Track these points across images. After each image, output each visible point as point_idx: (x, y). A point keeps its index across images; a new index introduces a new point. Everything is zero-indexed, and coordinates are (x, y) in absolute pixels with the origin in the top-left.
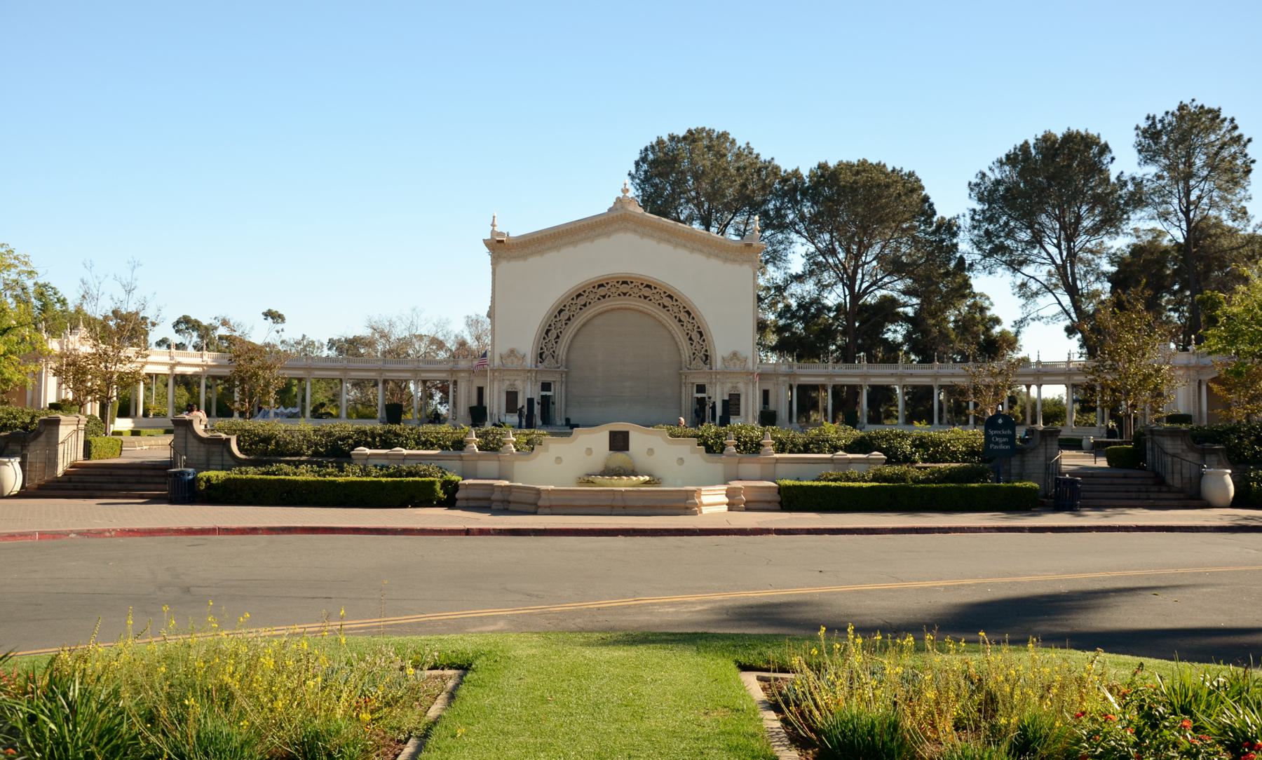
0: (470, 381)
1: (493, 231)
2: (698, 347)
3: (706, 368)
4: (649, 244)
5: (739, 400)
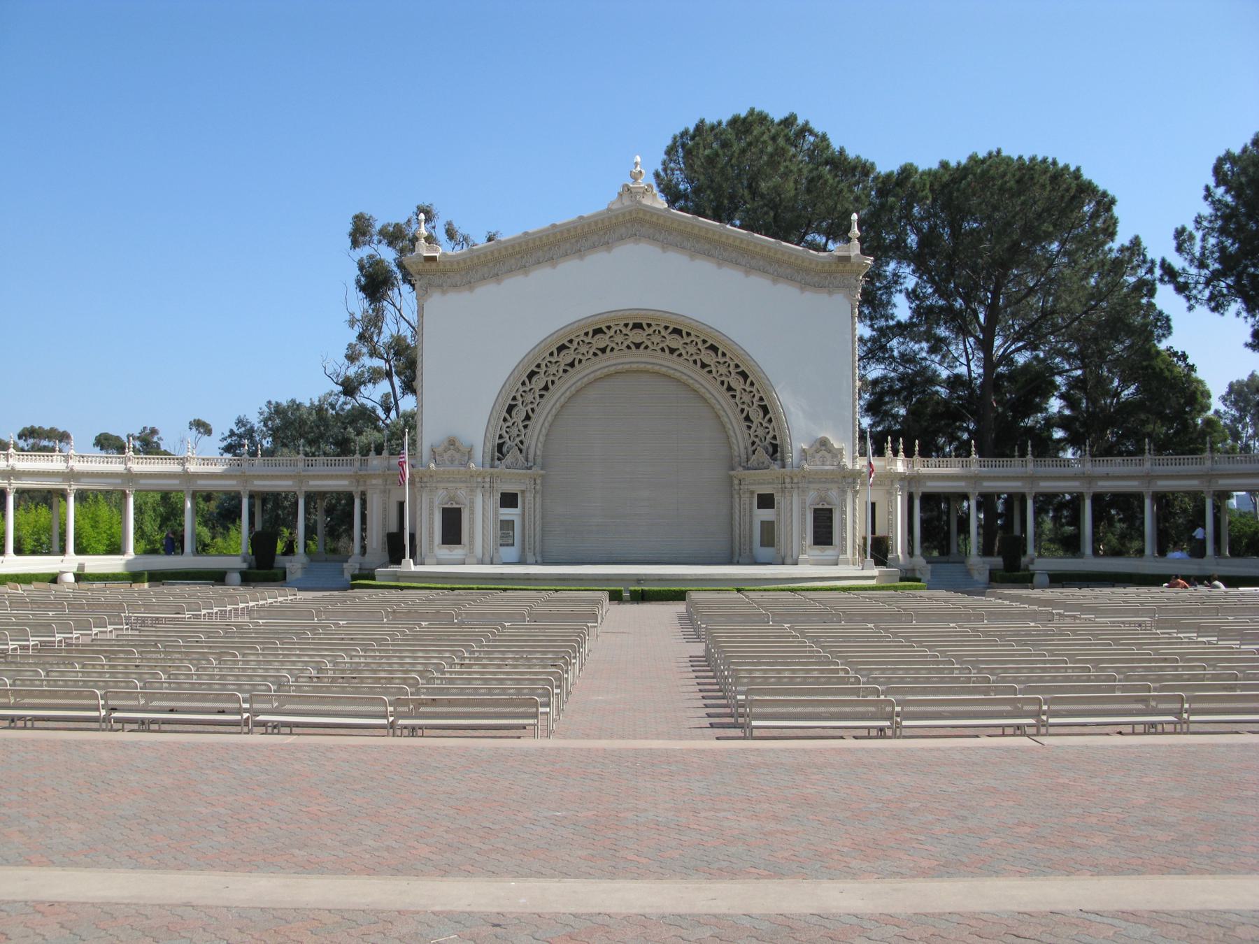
0: (385, 492)
2: (761, 432)
3: (776, 467)
4: (676, 261)
5: (830, 519)
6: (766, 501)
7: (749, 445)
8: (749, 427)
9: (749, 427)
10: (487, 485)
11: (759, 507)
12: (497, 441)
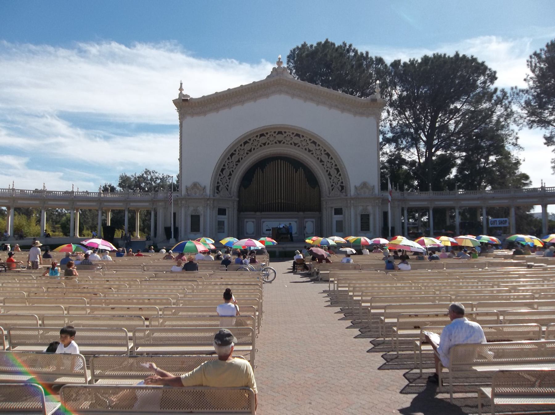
1: (181, 94)
2: (336, 180)
5: (369, 219)
6: (338, 211)
7: (330, 186)
8: (330, 178)
9: (330, 178)
10: (211, 205)
11: (335, 214)
12: (216, 185)
